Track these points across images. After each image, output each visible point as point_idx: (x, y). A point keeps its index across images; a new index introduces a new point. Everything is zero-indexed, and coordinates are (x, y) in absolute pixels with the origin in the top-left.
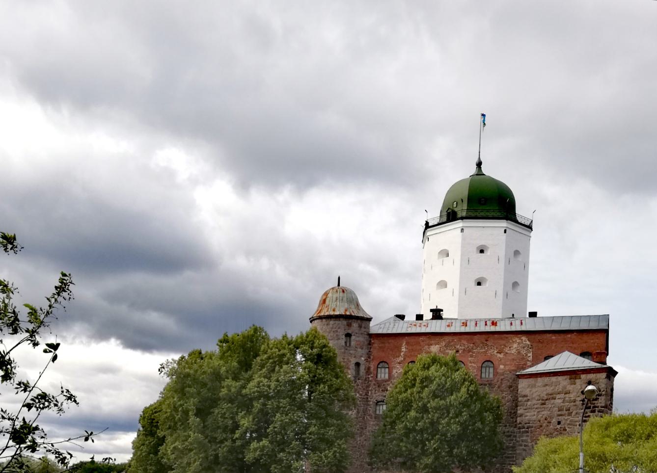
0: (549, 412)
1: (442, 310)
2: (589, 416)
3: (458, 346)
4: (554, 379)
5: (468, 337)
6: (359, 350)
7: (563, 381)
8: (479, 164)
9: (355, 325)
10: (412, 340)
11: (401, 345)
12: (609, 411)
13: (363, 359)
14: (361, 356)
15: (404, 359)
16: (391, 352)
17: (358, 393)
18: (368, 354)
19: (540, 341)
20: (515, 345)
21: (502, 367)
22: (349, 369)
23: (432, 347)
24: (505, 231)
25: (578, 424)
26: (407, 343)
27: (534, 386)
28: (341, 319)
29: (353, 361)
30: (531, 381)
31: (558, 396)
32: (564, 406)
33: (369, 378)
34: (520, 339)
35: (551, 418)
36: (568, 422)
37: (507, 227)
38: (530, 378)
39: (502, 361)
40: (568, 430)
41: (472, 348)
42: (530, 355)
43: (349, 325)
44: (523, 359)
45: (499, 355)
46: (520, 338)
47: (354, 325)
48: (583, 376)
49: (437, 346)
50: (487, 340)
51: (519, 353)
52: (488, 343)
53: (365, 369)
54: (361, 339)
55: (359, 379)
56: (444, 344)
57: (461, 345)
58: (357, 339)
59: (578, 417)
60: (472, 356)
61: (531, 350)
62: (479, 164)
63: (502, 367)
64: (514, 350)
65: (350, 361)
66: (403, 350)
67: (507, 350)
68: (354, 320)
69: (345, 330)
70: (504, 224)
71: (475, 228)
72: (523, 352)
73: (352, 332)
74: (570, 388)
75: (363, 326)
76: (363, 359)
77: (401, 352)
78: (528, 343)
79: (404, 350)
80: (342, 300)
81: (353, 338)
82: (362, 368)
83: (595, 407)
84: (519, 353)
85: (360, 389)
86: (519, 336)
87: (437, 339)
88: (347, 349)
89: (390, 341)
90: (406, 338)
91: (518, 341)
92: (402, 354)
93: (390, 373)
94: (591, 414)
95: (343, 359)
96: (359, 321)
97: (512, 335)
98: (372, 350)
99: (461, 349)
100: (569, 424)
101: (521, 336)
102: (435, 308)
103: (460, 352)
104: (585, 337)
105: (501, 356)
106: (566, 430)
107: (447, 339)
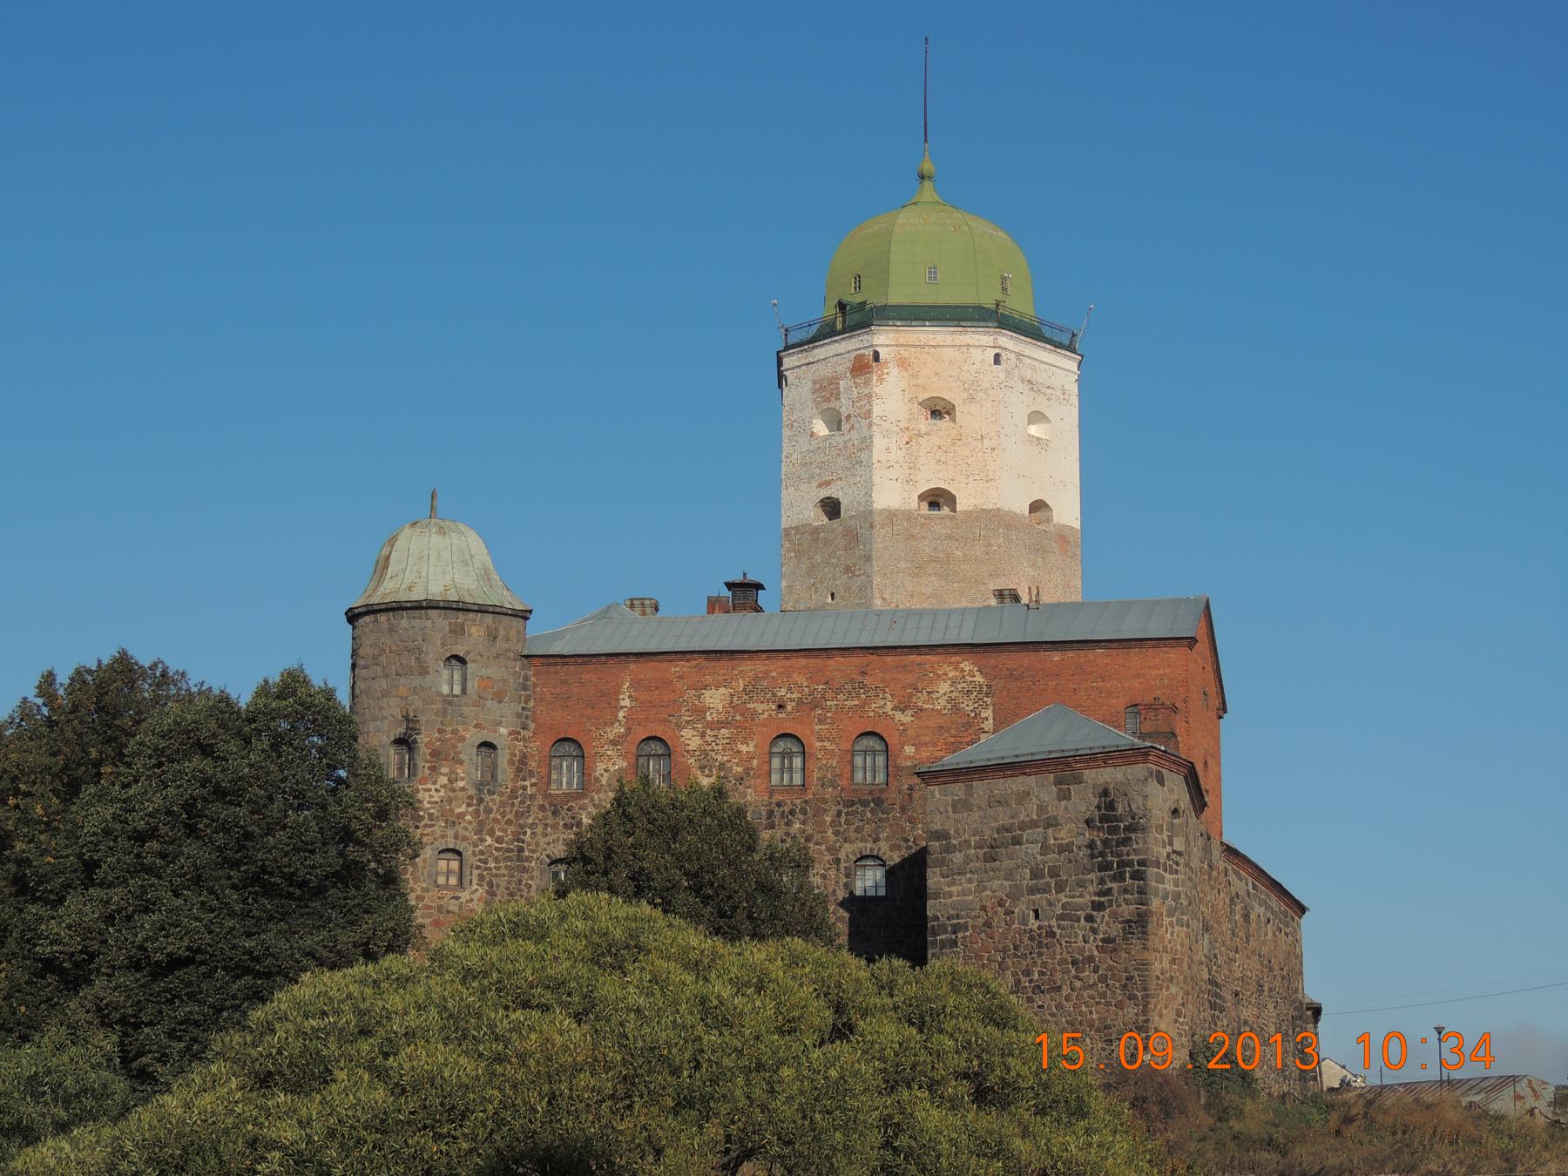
0: (1006, 883)
1: (759, 587)
2: (1109, 892)
3: (783, 691)
4: (1018, 784)
5: (812, 662)
6: (490, 704)
7: (1041, 790)
9: (476, 629)
10: (648, 670)
11: (617, 691)
12: (1167, 875)
13: (503, 731)
14: (499, 724)
15: (629, 730)
17: (491, 833)
18: (519, 716)
19: (1011, 675)
20: (944, 687)
21: (909, 750)
22: (461, 762)
23: (707, 693)
25: (1082, 914)
26: (636, 684)
27: (961, 806)
29: (473, 737)
30: (958, 790)
31: (1026, 835)
32: (1044, 863)
33: (524, 788)
34: (956, 669)
35: (1014, 897)
36: (1059, 911)
38: (955, 782)
39: (910, 732)
40: (1058, 932)
41: (823, 697)
42: (988, 713)
43: (458, 631)
44: (969, 725)
45: (898, 716)
46: (956, 666)
47: (474, 629)
48: (1090, 775)
49: (722, 690)
51: (956, 708)
52: (867, 680)
53: (511, 762)
54: (496, 672)
55: (490, 793)
57: (789, 689)
58: (485, 672)
59: (1081, 896)
60: (822, 721)
61: (989, 700)
63: (909, 750)
64: (942, 702)
65: (463, 739)
66: (623, 703)
67: (920, 700)
68: (471, 615)
69: (443, 645)
72: (968, 706)
73: (468, 653)
74: (1058, 809)
75: (502, 633)
76: (503, 731)
78: (979, 678)
81: (471, 667)
82: (503, 757)
83: (1122, 864)
84: (956, 708)
85: (495, 820)
88: (450, 703)
89: (584, 677)
90: (633, 667)
91: (951, 675)
92: (621, 715)
93: (584, 773)
94: (1114, 885)
95: (440, 731)
97: (933, 658)
98: (531, 704)
99: (791, 700)
100: (1060, 918)
101: (958, 658)
102: (738, 578)
103: (789, 708)
105: (906, 718)
106: (1052, 934)
107: (748, 667)
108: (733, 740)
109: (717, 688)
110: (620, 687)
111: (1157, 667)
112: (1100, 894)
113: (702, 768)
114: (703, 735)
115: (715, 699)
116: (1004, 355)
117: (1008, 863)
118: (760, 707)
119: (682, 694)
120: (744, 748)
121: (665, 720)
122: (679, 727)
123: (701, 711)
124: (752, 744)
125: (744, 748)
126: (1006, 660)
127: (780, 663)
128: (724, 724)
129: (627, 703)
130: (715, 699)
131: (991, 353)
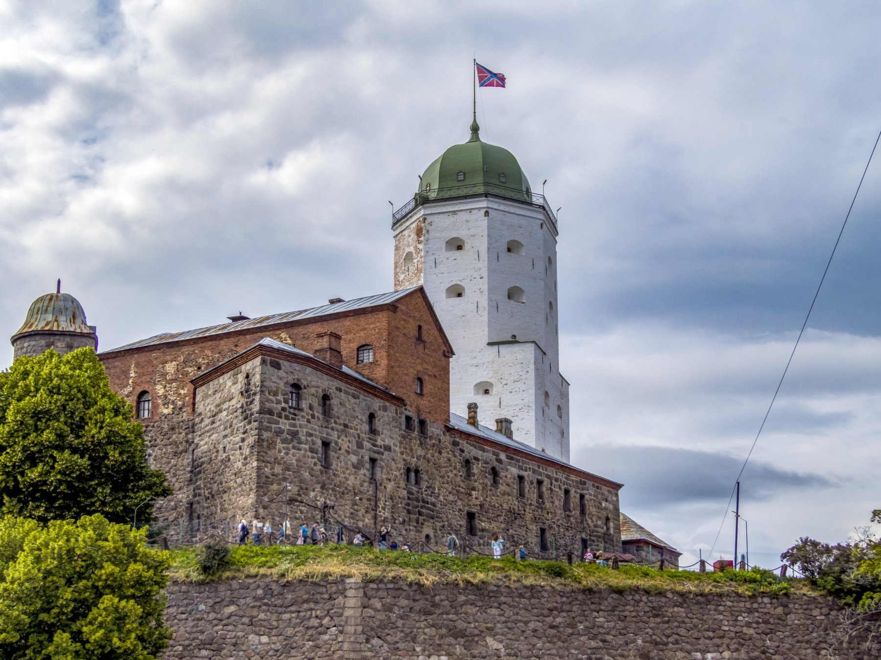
8: (475, 129)
10: (142, 358)
11: (129, 370)
16: (117, 381)
23: (167, 365)
24: (487, 213)
26: (137, 365)
28: (37, 338)
37: (488, 207)
49: (174, 363)
50: (236, 346)
56: (182, 358)
62: (475, 129)
68: (57, 337)
70: (483, 203)
71: (442, 215)
77: (128, 378)
79: (133, 375)
80: (46, 310)
86: (278, 332)
87: (173, 352)
89: (116, 364)
92: (131, 381)
96: (68, 339)
104: (362, 320)
107: (186, 350)
108: (178, 388)
109: (172, 361)
110: (130, 367)
111: (373, 323)
112: (244, 433)
113: (164, 405)
114: (165, 387)
115: (170, 368)
116: (490, 211)
117: (218, 424)
118: (190, 370)
119: (157, 367)
120: (182, 392)
121: (149, 382)
122: (155, 384)
123: (164, 375)
124: (186, 389)
125: (182, 392)
126: (301, 330)
127: (200, 345)
128: (175, 380)
129: (133, 375)
130: (170, 368)
131: (483, 211)
